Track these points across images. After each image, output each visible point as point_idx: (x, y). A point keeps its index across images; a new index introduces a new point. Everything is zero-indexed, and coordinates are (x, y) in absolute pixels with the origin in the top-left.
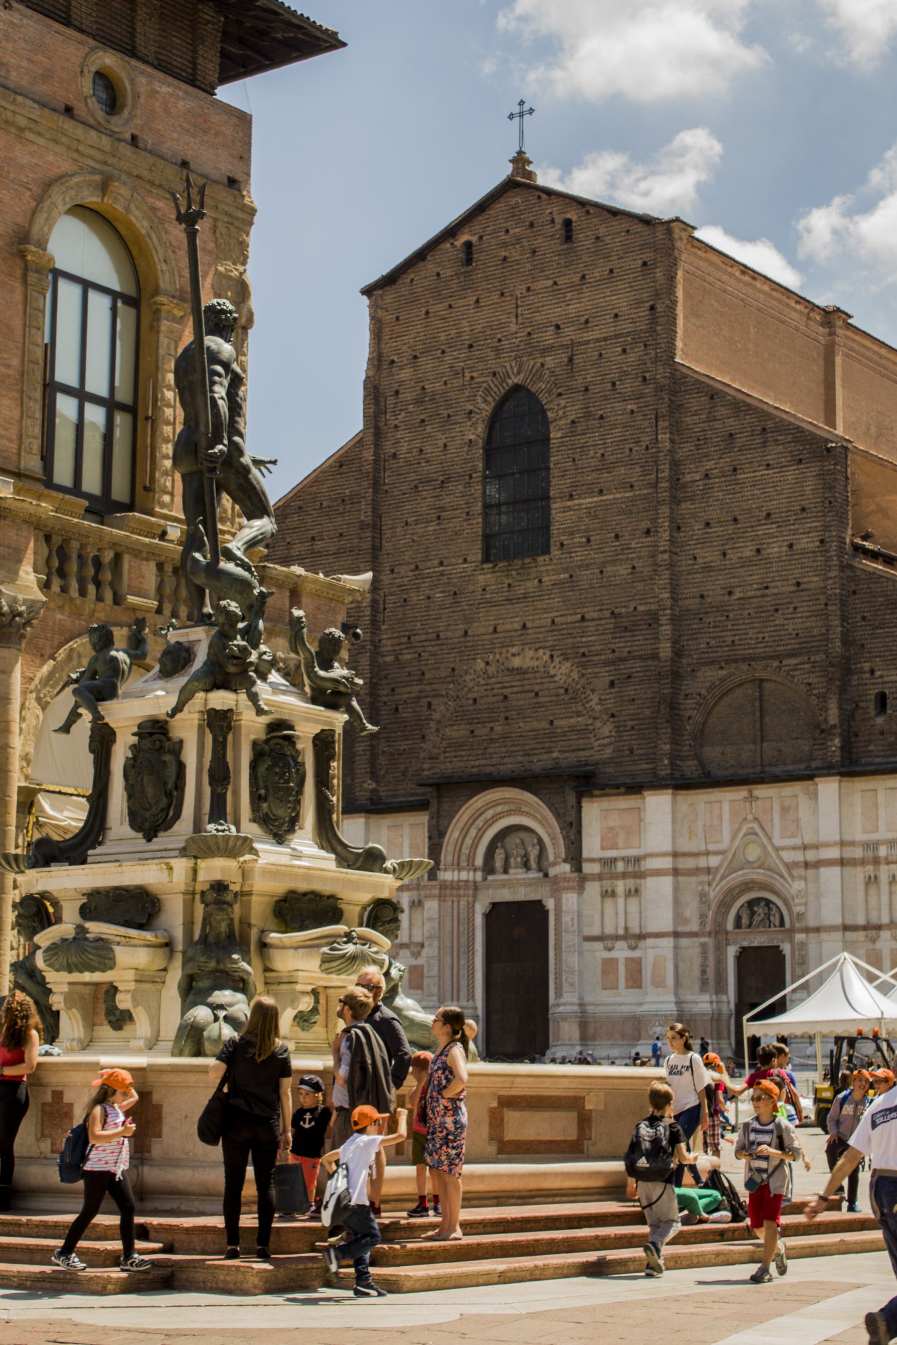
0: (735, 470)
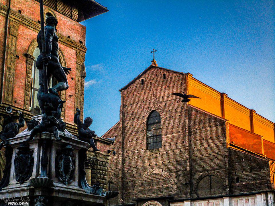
0: (203, 128)
